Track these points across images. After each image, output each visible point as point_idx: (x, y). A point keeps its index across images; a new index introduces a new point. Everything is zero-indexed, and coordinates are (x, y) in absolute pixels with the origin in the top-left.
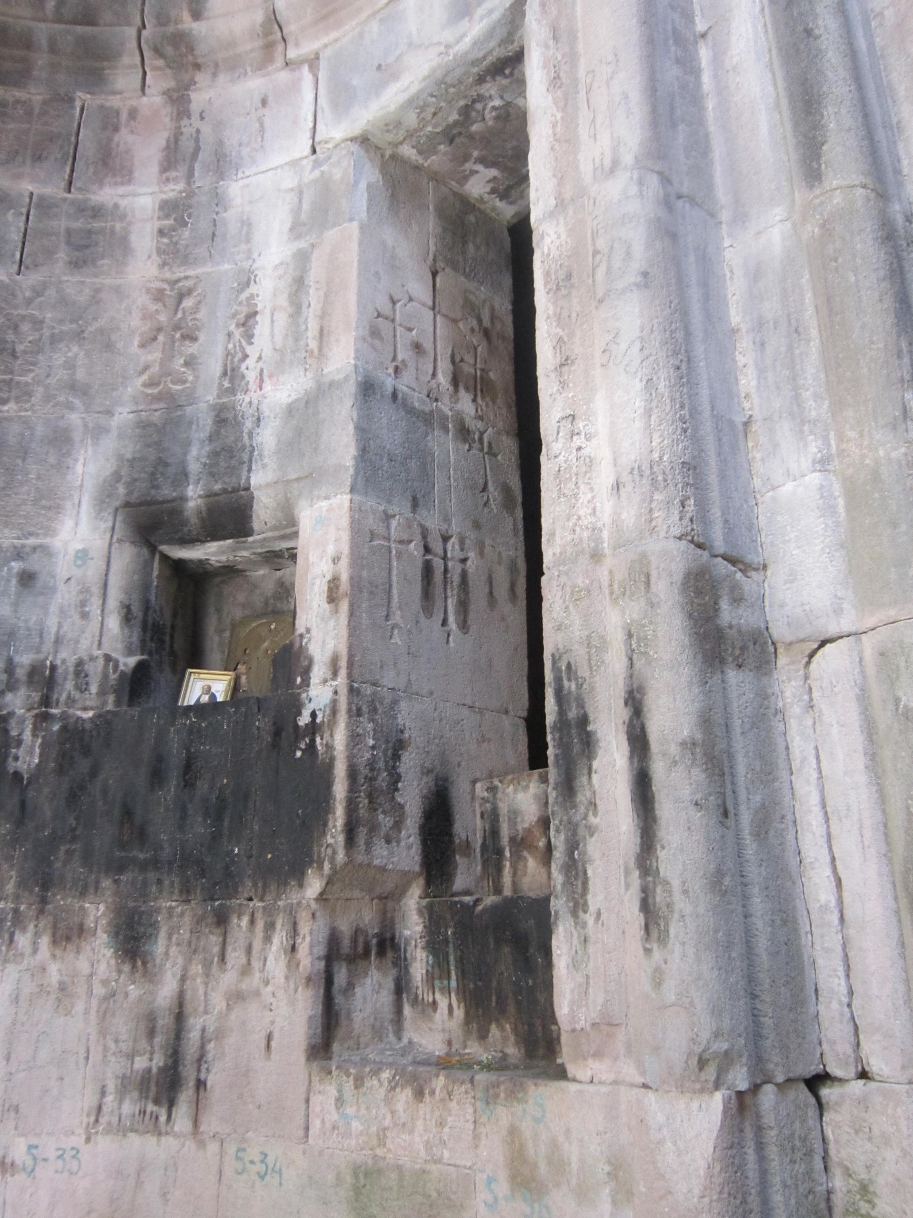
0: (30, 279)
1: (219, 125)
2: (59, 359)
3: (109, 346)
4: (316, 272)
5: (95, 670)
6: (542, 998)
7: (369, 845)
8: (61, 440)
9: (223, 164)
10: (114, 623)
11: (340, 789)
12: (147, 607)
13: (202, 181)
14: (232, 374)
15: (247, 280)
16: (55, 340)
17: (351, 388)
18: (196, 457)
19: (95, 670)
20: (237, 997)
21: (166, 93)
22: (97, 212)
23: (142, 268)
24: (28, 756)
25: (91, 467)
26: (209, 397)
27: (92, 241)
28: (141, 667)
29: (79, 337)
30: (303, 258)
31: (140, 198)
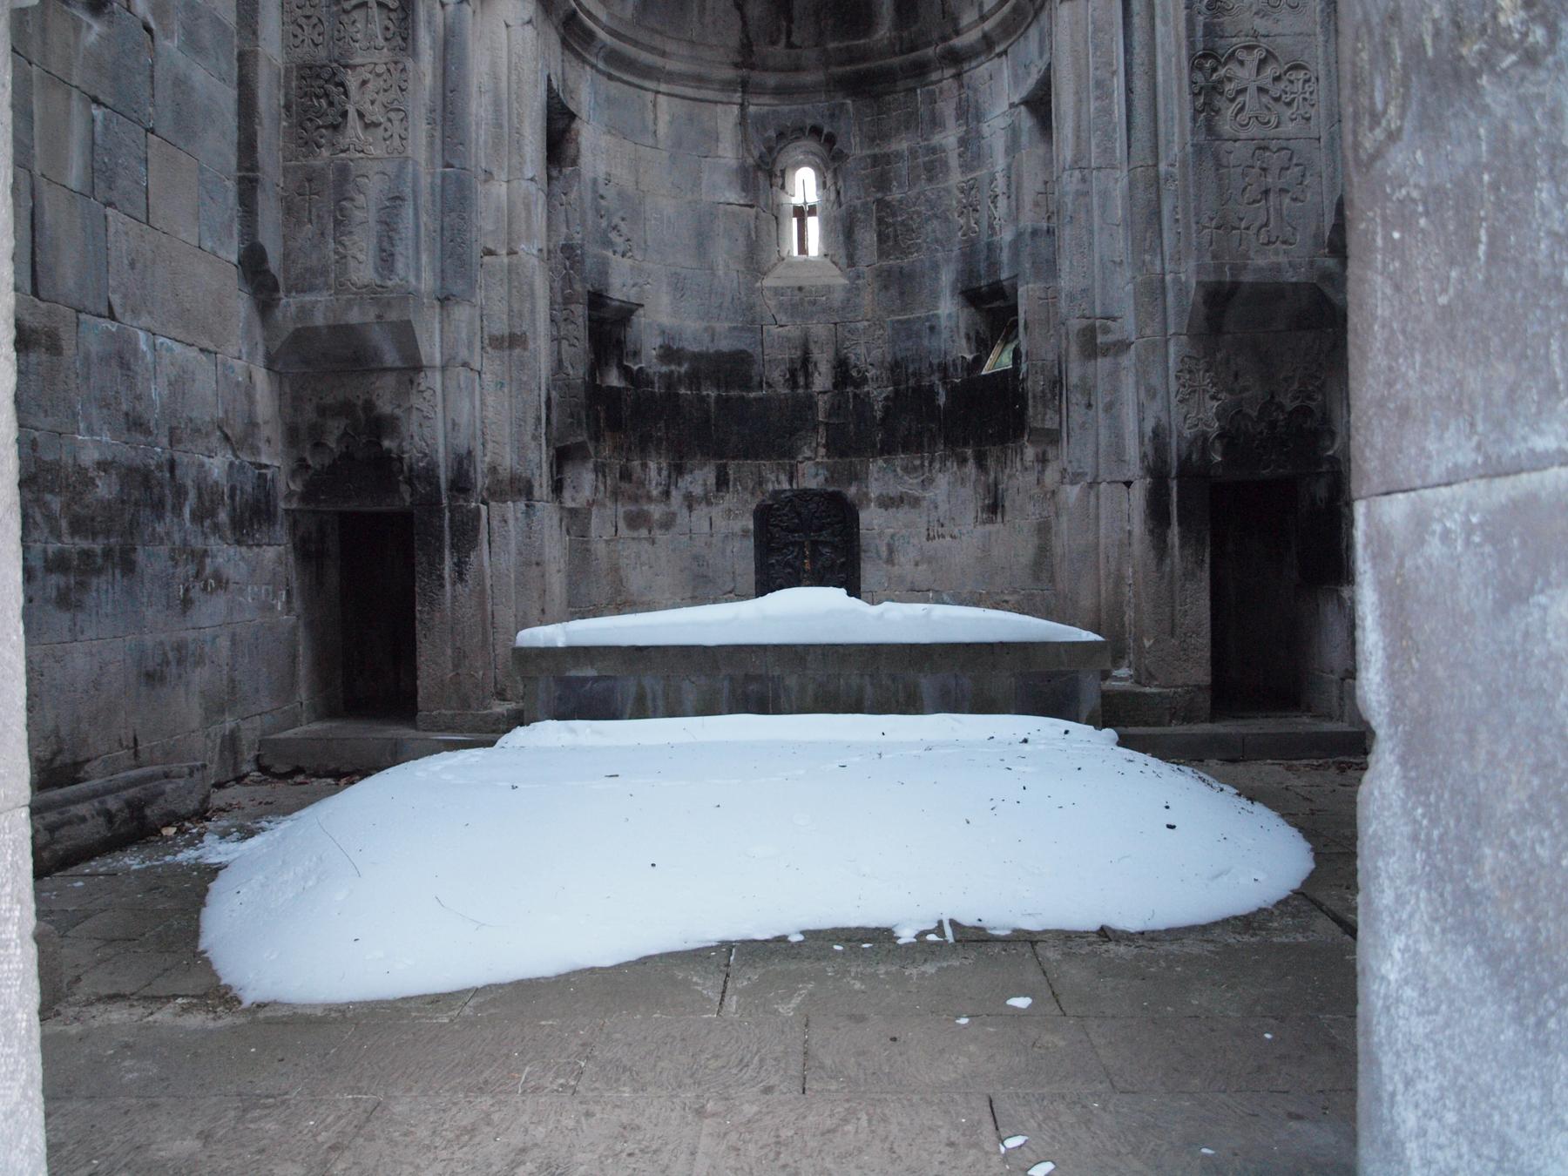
0: (916, 190)
1: (976, 90)
2: (929, 228)
3: (947, 219)
4: (1013, 177)
5: (959, 362)
6: (1345, 510)
7: (1043, 420)
8: (935, 267)
9: (979, 117)
10: (964, 342)
11: (1030, 402)
12: (978, 333)
13: (973, 124)
14: (991, 227)
15: (993, 180)
16: (928, 219)
17: (1027, 236)
18: (983, 266)
19: (959, 362)
20: (1010, 477)
21: (953, 76)
22: (933, 150)
23: (956, 178)
24: (942, 400)
25: (947, 277)
26: (985, 239)
27: (934, 167)
28: (975, 359)
29: (936, 216)
30: (1009, 167)
31: (949, 138)
